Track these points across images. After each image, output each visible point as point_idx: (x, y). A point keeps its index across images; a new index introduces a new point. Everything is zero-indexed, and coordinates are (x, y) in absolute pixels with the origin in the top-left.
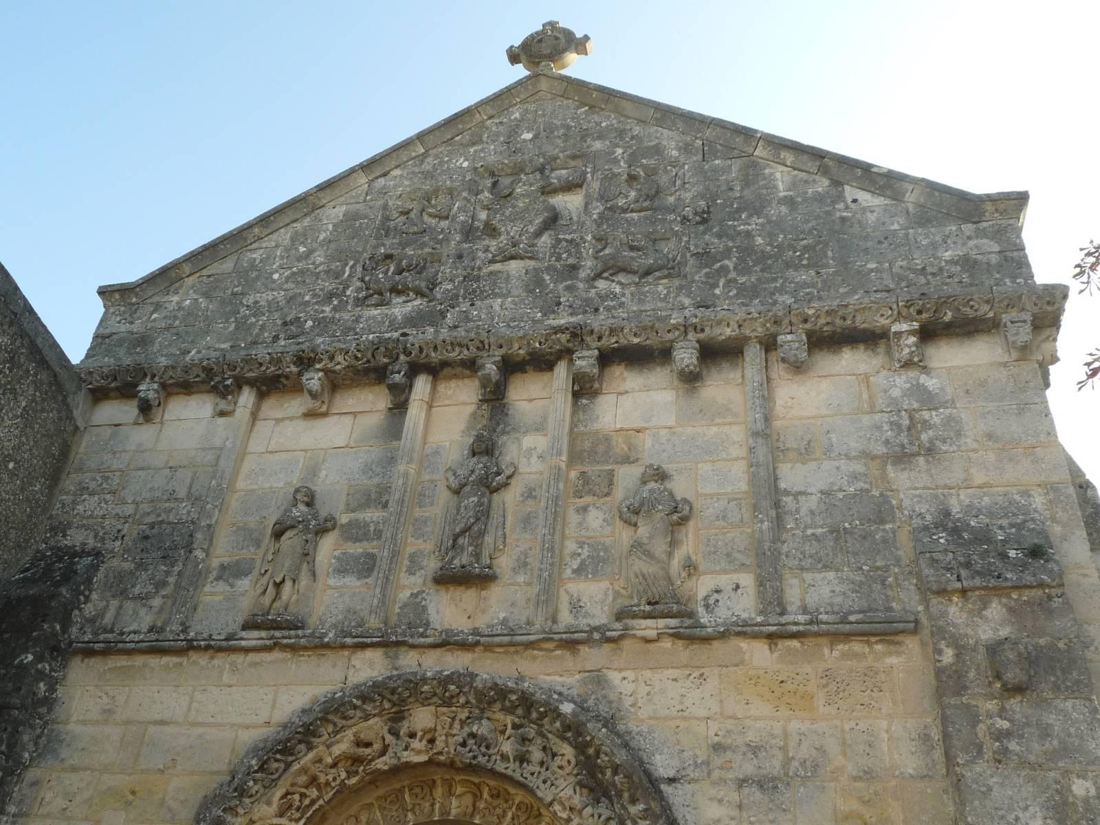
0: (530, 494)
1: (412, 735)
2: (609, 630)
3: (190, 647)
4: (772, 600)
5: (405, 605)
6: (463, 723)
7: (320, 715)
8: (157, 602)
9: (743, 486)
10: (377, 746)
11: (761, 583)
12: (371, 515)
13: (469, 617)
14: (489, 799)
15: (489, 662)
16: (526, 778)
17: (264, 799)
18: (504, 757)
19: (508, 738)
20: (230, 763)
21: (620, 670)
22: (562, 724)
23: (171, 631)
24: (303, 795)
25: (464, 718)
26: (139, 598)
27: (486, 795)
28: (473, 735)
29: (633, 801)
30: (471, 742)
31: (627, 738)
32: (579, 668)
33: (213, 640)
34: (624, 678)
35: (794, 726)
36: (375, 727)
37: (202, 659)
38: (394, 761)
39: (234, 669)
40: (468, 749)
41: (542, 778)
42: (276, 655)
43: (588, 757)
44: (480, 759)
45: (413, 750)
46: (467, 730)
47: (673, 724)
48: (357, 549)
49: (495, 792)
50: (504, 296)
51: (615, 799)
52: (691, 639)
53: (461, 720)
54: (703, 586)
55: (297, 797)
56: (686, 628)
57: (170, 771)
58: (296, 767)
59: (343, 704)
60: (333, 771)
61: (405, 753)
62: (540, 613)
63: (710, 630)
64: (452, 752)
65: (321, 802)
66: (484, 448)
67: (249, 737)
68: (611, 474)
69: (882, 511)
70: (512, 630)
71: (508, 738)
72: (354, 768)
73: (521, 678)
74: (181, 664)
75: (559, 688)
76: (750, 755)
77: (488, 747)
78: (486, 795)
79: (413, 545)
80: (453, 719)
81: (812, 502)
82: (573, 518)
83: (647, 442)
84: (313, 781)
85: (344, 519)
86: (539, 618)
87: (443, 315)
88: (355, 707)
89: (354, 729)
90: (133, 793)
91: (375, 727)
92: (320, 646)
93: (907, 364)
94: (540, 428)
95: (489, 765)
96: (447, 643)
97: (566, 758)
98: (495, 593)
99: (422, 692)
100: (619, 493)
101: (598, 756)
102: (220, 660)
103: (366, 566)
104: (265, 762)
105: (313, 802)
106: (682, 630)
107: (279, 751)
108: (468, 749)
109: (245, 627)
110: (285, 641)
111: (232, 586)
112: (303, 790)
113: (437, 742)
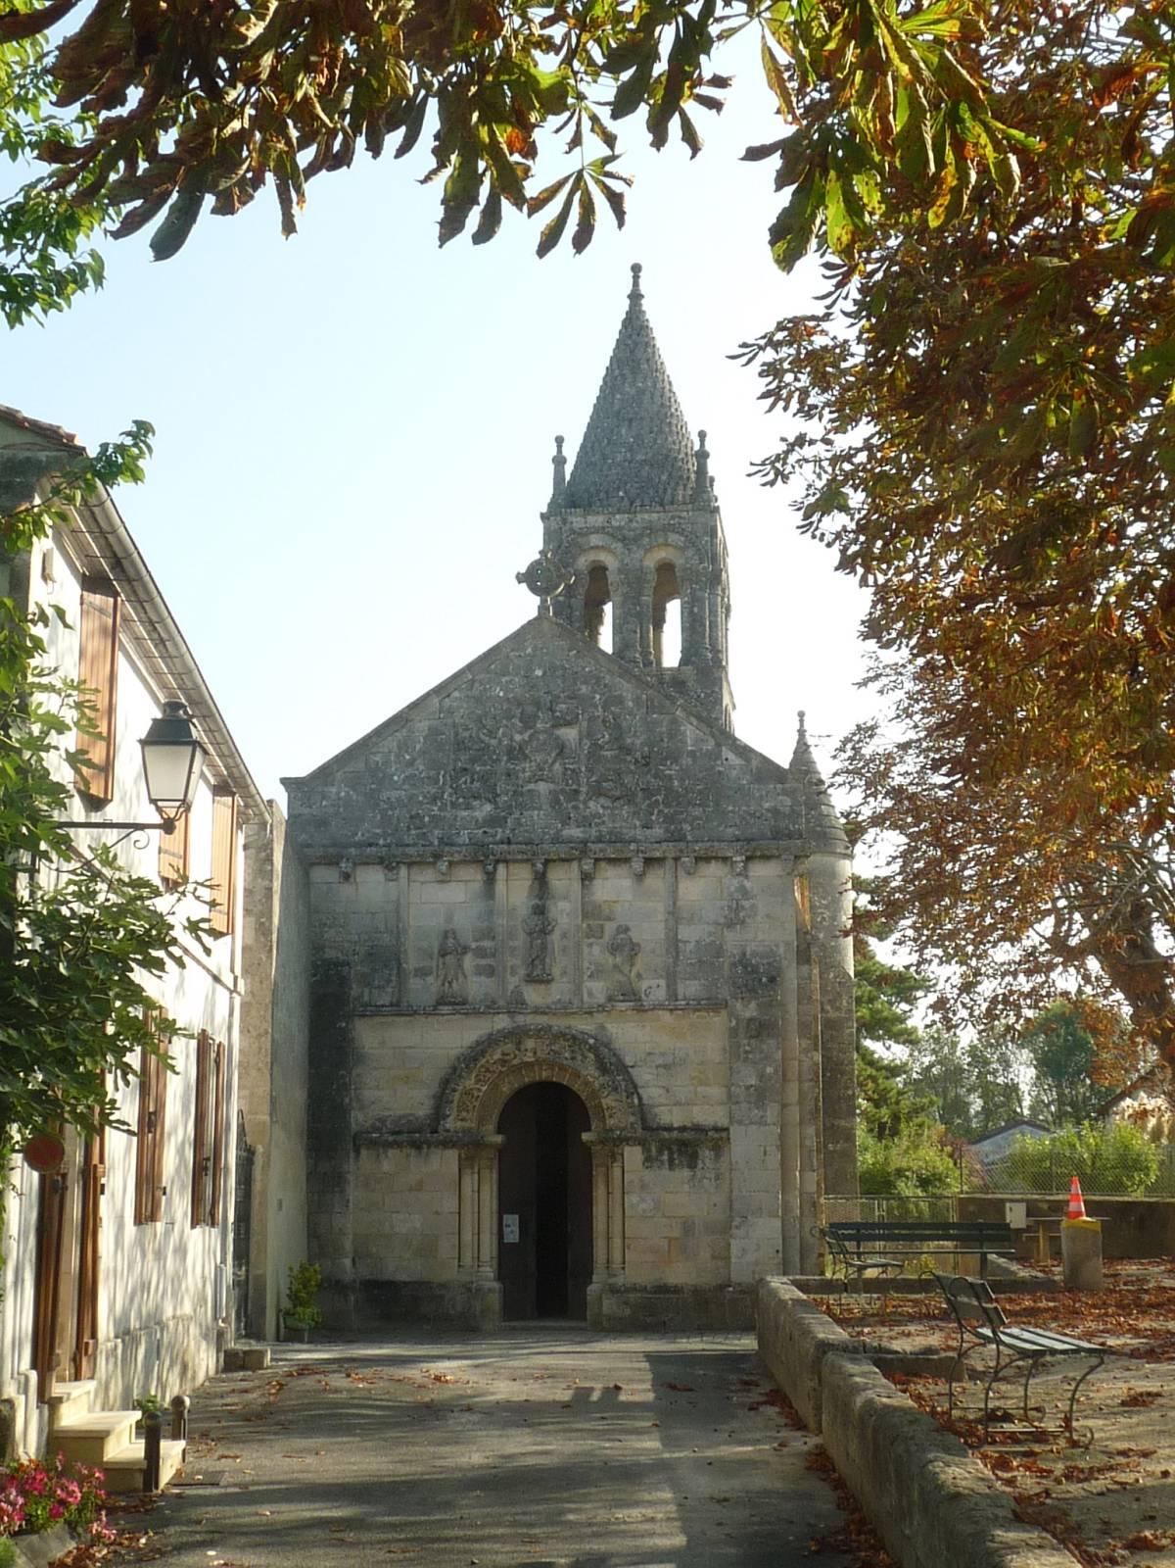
0: (564, 936)
4: (673, 995)
8: (390, 990)
9: (663, 936)
11: (668, 986)
12: (487, 944)
26: (379, 987)
35: (678, 1045)
36: (509, 1047)
42: (457, 1017)
48: (483, 962)
50: (540, 809)
52: (638, 1011)
54: (644, 985)
66: (540, 911)
68: (602, 927)
69: (719, 951)
79: (511, 962)
81: (691, 946)
82: (586, 950)
83: (618, 908)
84: (488, 1070)
85: (474, 945)
87: (505, 818)
91: (509, 1047)
92: (477, 1013)
93: (739, 874)
94: (566, 898)
98: (554, 986)
100: (607, 937)
103: (490, 972)
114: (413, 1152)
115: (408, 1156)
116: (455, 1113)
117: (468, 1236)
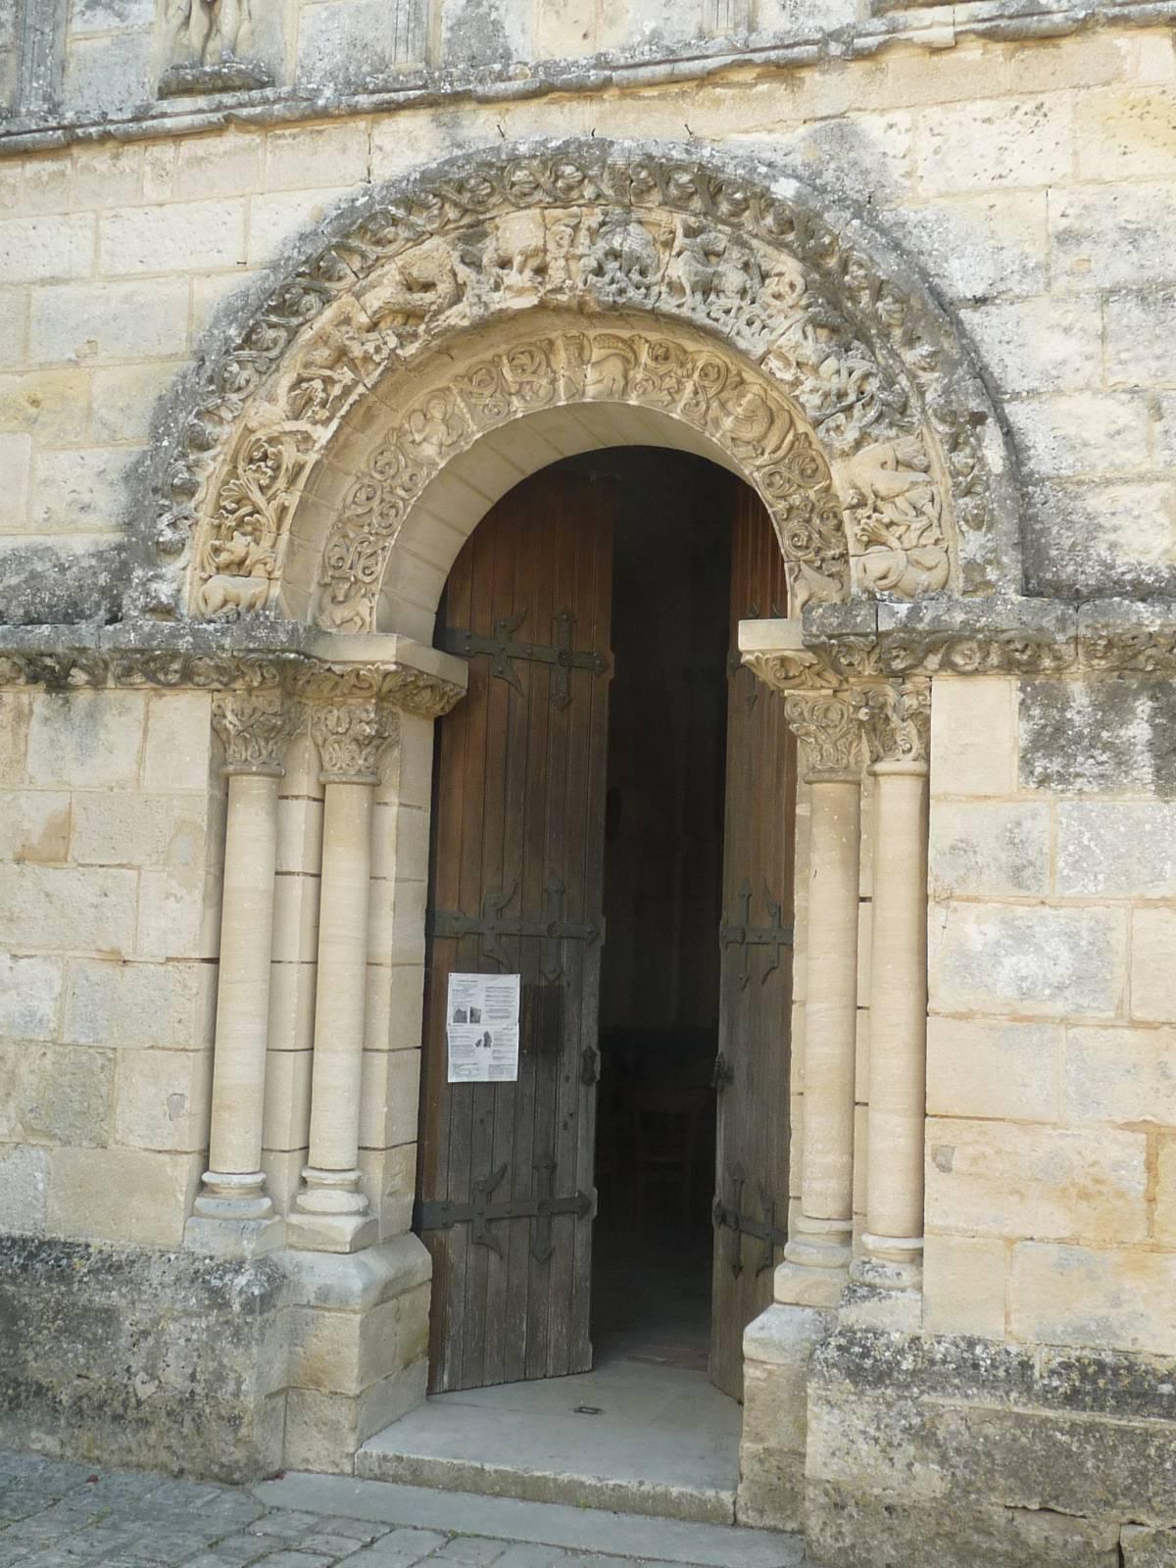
1: (505, 264)
2: (860, 35)
3: (72, 140)
5: (460, 23)
6: (593, 234)
7: (334, 241)
10: (445, 287)
13: (585, 36)
14: (651, 364)
15: (631, 117)
16: (717, 320)
17: (262, 392)
18: (675, 288)
19: (679, 254)
20: (190, 339)
21: (883, 111)
22: (778, 219)
23: (30, 113)
24: (328, 381)
25: (595, 225)
27: (644, 358)
28: (615, 255)
29: (911, 341)
30: (612, 266)
31: (899, 235)
32: (804, 114)
33: (112, 122)
34: (891, 126)
36: (436, 255)
37: (98, 160)
38: (478, 311)
39: (161, 173)
40: (607, 278)
41: (745, 317)
42: (232, 139)
43: (827, 274)
44: (631, 293)
45: (509, 288)
46: (602, 245)
47: (982, 202)
49: (660, 352)
51: (878, 343)
53: (589, 229)
55: (318, 384)
56: (1011, 17)
57: (89, 361)
58: (306, 335)
59: (373, 217)
60: (373, 336)
61: (497, 296)
62: (723, 13)
63: (1058, 18)
64: (581, 285)
65: (361, 389)
67: (217, 290)
70: (673, 52)
71: (679, 254)
72: (409, 329)
73: (695, 142)
74: (63, 174)
75: (768, 155)
76: (1125, 247)
77: (643, 273)
78: (644, 358)
80: (576, 228)
84: (342, 355)
86: (723, 24)
88: (395, 222)
89: (399, 261)
90: (35, 403)
91: (436, 255)
92: (315, 116)
95: (649, 304)
96: (548, 88)
97: (786, 279)
99: (513, 184)
101: (844, 268)
102: (133, 158)
104: (253, 330)
105: (347, 390)
106: (1003, 23)
107: (272, 310)
108: (607, 278)
109: (164, 93)
110: (245, 112)
111: (121, 16)
112: (328, 373)
113: (550, 271)
114: (38, 699)
115: (22, 716)
116: (201, 538)
117: (239, 1066)
